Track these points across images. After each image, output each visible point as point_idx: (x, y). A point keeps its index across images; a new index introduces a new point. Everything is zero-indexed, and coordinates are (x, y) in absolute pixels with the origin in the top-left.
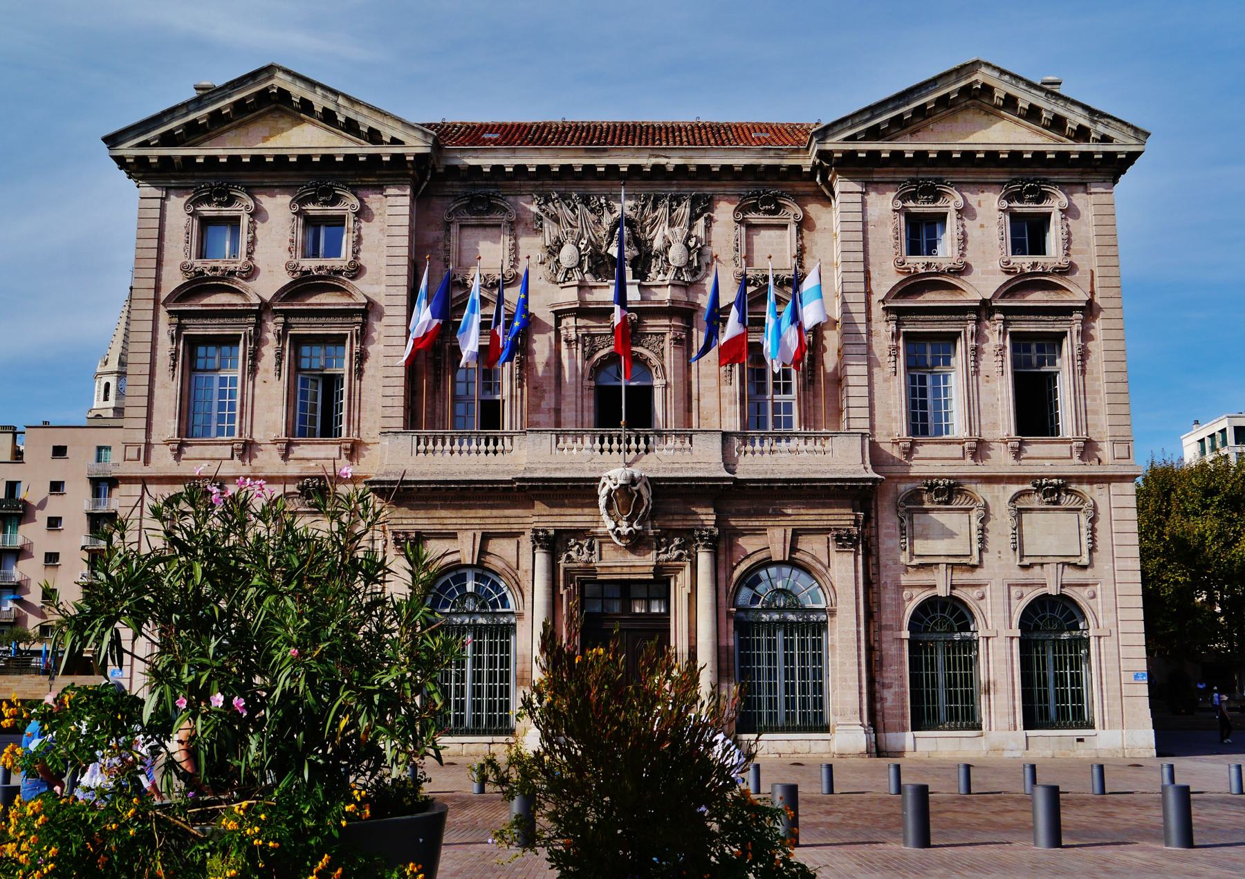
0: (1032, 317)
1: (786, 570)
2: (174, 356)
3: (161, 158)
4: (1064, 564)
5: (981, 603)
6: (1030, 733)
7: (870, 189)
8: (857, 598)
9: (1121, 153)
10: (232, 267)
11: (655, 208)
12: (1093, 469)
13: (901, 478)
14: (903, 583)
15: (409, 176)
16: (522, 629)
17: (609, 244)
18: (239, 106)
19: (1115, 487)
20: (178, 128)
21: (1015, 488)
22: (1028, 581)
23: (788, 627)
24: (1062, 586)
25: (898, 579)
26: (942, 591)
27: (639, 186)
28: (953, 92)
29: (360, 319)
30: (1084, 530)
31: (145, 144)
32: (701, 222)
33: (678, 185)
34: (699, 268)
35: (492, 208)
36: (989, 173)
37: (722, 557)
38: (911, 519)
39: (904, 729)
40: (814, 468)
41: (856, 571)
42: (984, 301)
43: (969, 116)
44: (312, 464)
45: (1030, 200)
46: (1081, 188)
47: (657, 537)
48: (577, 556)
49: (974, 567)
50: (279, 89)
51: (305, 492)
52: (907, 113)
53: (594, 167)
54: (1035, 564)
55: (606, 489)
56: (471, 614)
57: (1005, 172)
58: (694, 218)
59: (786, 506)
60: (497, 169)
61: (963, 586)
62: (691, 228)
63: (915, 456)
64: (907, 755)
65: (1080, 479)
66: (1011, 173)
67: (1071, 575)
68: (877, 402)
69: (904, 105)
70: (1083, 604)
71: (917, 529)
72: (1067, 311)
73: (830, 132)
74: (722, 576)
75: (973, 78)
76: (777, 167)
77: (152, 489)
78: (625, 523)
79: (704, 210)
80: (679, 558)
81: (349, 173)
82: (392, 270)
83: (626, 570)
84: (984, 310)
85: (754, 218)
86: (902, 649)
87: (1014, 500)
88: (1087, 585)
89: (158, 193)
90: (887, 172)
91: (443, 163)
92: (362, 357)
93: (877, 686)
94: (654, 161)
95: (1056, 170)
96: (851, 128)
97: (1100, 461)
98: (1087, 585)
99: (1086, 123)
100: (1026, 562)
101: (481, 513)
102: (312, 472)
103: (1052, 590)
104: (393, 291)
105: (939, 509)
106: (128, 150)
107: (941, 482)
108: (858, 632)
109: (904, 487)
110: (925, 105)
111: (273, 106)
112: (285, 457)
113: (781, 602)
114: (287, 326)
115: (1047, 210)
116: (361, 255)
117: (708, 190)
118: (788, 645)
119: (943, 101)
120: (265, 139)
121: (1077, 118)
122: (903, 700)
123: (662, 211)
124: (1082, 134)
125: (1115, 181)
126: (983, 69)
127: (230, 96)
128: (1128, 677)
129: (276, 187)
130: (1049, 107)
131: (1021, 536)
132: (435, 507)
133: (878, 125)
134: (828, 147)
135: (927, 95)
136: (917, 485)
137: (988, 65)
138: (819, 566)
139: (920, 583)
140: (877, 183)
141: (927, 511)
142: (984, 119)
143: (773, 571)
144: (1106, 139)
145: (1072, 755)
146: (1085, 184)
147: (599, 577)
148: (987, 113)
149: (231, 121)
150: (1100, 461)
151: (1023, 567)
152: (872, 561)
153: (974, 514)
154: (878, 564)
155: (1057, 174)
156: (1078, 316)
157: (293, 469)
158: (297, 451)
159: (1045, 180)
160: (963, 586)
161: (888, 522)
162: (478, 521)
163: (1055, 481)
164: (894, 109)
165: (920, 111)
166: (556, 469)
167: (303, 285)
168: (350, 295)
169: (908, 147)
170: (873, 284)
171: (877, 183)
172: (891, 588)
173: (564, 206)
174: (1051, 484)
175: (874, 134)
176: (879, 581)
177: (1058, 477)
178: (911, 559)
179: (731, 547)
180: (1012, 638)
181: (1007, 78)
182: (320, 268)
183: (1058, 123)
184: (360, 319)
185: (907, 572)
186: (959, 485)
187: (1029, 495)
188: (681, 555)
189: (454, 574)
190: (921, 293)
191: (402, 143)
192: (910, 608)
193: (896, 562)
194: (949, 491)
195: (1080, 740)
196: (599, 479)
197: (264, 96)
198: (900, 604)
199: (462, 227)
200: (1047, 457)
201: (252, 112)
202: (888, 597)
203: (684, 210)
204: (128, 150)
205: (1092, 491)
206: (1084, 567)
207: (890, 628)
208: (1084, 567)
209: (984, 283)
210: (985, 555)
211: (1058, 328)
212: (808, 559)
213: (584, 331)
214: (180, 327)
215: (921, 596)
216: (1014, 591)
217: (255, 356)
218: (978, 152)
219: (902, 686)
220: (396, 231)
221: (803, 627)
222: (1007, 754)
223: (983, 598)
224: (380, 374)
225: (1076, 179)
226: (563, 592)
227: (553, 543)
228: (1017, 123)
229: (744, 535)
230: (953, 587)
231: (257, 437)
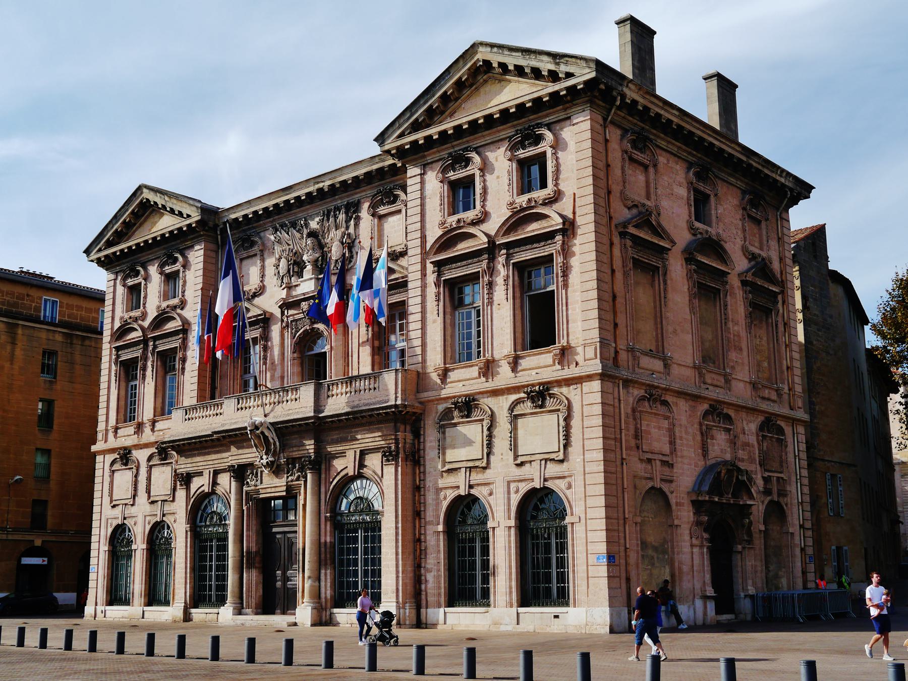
0: (528, 247)
4: (546, 460)
5: (491, 499)
6: (521, 610)
8: (396, 501)
9: (579, 84)
11: (328, 220)
12: (571, 372)
13: (437, 400)
14: (440, 486)
15: (201, 236)
19: (587, 386)
21: (514, 397)
22: (522, 478)
24: (545, 480)
25: (436, 483)
27: (320, 205)
28: (463, 75)
30: (561, 428)
31: (100, 250)
32: (352, 222)
33: (341, 198)
35: (253, 244)
36: (499, 131)
37: (323, 476)
38: (444, 433)
39: (439, 607)
40: (366, 402)
41: (396, 479)
43: (488, 88)
45: (530, 145)
46: (568, 122)
48: (252, 484)
49: (485, 468)
52: (434, 103)
54: (526, 462)
57: (509, 127)
58: (347, 221)
59: (357, 432)
62: (347, 228)
63: (448, 380)
64: (439, 627)
65: (560, 383)
66: (514, 126)
67: (552, 469)
68: (428, 340)
69: (431, 98)
71: (448, 440)
72: (548, 236)
73: (386, 136)
74: (323, 490)
75: (475, 59)
76: (382, 168)
77: (107, 456)
79: (354, 212)
80: (298, 479)
85: (382, 210)
86: (438, 540)
87: (511, 409)
88: (564, 477)
90: (434, 153)
91: (221, 221)
93: (423, 571)
94: (317, 186)
95: (544, 113)
96: (399, 128)
97: (577, 364)
98: (564, 477)
99: (552, 67)
100: (518, 462)
101: (214, 457)
105: (463, 423)
107: (460, 400)
108: (397, 528)
109: (441, 407)
112: (153, 430)
114: (155, 347)
116: (186, 293)
117: (356, 197)
120: (150, 230)
121: (546, 65)
122: (439, 582)
123: (331, 219)
124: (554, 76)
126: (481, 49)
127: (127, 210)
128: (592, 559)
130: (527, 62)
131: (516, 439)
132: (194, 455)
133: (417, 119)
134: (386, 147)
135: (446, 84)
136: (449, 405)
137: (481, 44)
139: (450, 485)
141: (455, 425)
142: (498, 86)
145: (548, 630)
148: (500, 81)
150: (577, 364)
151: (517, 465)
153: (485, 423)
154: (424, 472)
155: (547, 116)
156: (559, 238)
157: (153, 439)
159: (538, 124)
160: (478, 485)
161: (431, 436)
162: (211, 463)
163: (537, 388)
164: (425, 103)
165: (445, 98)
169: (448, 125)
171: (432, 163)
172: (432, 490)
173: (283, 232)
175: (416, 127)
176: (425, 485)
177: (540, 384)
178: (444, 466)
179: (329, 467)
180: (510, 527)
181: (495, 50)
183: (537, 74)
185: (442, 476)
186: (474, 400)
188: (299, 476)
190: (455, 244)
192: (445, 504)
193: (436, 469)
194: (467, 406)
195: (556, 617)
198: (438, 504)
199: (241, 260)
200: (540, 366)
202: (430, 497)
203: (342, 217)
204: (94, 256)
205: (569, 392)
207: (431, 523)
208: (562, 461)
210: (492, 458)
213: (291, 319)
214: (118, 356)
215: (451, 495)
216: (513, 485)
218: (478, 119)
219: (439, 570)
222: (503, 628)
223: (491, 494)
225: (562, 115)
226: (245, 508)
227: (240, 473)
228: (519, 82)
229: (337, 457)
230: (471, 487)
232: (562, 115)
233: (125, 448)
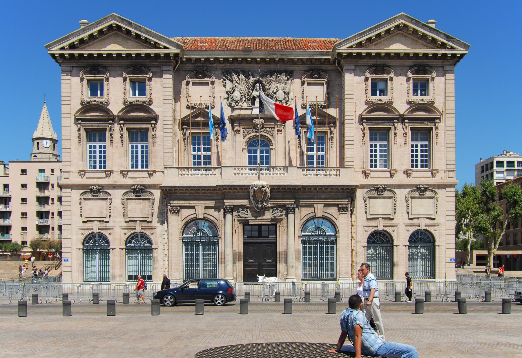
1: (321, 220)
2: (79, 137)
3: (70, 54)
7: (357, 68)
10: (101, 100)
16: (221, 243)
17: (253, 90)
18: (101, 32)
20: (76, 41)
22: (413, 225)
23: (321, 242)
26: (381, 228)
29: (153, 122)
34: (288, 101)
42: (400, 115)
44: (138, 180)
46: (441, 69)
47: (272, 208)
49: (392, 219)
50: (117, 25)
51: (135, 191)
53: (246, 59)
55: (253, 190)
56: (201, 237)
60: (207, 60)
61: (388, 226)
70: (433, 232)
78: (260, 203)
81: (147, 61)
82: (166, 102)
83: (260, 221)
84: (402, 119)
89: (69, 69)
92: (154, 137)
95: (432, 61)
102: (138, 183)
103: (423, 228)
104: (167, 110)
106: (56, 50)
107: (381, 187)
110: (380, 33)
111: (114, 32)
113: (318, 232)
115: (427, 77)
116: (152, 95)
118: (322, 248)
119: (388, 31)
125: (455, 65)
129: (118, 66)
138: (334, 219)
140: (360, 66)
143: (316, 220)
144: (452, 48)
146: (443, 67)
147: (250, 223)
148: (405, 36)
149: (97, 38)
152: (353, 216)
157: (130, 182)
158: (130, 175)
160: (388, 226)
163: (425, 186)
166: (233, 182)
167: (131, 107)
168: (150, 112)
169: (373, 51)
170: (357, 107)
171: (360, 66)
174: (424, 187)
177: (426, 185)
182: (137, 101)
184: (153, 122)
187: (415, 191)
189: (194, 222)
191: (168, 48)
196: (250, 186)
197: (110, 27)
201: (107, 34)
206: (434, 219)
208: (434, 219)
209: (401, 107)
211: (429, 125)
212: (330, 216)
217: (111, 136)
220: (167, 85)
221: (327, 242)
224: (162, 144)
228: (417, 41)
231: (114, 169)
232: (440, 64)
233: (99, 186)
